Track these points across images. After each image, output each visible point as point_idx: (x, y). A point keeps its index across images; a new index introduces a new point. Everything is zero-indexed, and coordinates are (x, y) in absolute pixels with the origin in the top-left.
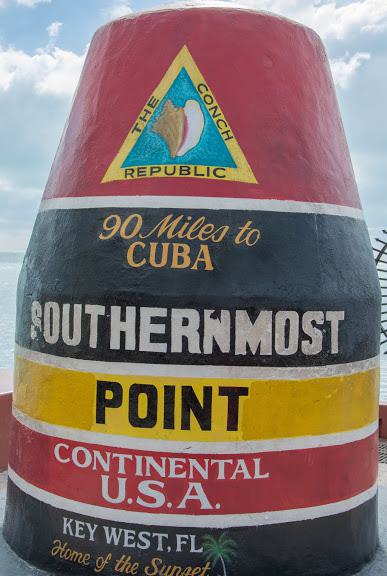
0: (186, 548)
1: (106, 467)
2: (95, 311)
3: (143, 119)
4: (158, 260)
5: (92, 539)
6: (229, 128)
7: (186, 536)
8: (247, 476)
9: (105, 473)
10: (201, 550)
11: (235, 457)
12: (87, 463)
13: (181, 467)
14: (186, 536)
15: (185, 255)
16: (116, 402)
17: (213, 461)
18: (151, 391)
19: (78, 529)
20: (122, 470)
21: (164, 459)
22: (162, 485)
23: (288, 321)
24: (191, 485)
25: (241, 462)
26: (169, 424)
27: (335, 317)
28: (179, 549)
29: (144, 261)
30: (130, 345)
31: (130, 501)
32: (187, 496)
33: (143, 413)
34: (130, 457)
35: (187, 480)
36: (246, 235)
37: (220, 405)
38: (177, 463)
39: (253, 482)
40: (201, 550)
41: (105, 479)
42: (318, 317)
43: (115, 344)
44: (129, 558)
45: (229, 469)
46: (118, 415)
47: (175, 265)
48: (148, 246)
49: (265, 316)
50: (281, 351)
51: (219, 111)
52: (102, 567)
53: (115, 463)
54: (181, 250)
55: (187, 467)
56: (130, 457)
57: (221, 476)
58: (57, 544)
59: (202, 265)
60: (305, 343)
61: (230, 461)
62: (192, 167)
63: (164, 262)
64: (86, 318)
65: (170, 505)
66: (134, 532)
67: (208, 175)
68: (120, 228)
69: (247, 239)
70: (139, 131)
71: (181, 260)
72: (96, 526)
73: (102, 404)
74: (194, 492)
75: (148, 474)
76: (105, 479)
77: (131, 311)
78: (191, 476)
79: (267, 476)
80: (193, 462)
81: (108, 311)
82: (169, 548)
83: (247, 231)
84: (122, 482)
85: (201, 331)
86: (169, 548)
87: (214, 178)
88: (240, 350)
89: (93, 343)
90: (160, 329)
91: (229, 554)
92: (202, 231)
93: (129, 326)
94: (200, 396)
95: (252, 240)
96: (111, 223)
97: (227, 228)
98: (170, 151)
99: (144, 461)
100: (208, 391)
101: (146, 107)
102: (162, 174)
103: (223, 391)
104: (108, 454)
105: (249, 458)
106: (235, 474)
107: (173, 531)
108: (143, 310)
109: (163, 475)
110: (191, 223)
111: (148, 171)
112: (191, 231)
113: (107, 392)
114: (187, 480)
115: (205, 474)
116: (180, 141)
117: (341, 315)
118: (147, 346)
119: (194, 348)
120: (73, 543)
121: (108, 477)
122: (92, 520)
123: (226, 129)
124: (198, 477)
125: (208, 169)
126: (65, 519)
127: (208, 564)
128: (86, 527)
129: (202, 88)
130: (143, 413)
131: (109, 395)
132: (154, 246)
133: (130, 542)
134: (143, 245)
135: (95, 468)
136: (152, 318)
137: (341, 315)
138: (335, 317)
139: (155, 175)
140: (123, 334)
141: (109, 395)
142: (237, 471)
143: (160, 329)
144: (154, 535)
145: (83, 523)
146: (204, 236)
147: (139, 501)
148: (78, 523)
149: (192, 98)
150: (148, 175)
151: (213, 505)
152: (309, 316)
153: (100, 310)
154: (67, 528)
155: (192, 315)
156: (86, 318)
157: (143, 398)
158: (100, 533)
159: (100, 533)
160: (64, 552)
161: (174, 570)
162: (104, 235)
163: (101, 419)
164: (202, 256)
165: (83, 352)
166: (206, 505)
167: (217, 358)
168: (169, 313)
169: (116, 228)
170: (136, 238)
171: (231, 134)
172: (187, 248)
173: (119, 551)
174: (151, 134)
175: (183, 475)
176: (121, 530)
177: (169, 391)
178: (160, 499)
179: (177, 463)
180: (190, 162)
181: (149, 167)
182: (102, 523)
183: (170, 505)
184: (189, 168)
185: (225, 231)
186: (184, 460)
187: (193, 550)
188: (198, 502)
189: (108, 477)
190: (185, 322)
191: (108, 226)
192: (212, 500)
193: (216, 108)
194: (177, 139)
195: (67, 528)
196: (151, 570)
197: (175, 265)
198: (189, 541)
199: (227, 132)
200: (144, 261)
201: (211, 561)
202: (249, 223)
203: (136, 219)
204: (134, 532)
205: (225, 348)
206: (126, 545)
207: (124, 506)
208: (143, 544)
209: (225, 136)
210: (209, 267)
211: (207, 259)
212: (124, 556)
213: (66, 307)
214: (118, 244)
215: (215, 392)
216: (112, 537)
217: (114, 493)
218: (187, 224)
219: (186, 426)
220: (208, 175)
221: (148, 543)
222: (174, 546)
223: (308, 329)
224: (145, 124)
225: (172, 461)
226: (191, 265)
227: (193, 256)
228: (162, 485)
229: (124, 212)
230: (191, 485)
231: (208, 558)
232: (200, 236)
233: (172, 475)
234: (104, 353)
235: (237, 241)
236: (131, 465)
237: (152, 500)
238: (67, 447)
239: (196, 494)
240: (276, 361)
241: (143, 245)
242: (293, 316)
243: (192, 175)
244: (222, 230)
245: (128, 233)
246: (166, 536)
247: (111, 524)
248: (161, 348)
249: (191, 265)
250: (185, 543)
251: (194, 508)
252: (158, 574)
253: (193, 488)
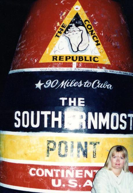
2: (46, 113)
64: (42, 117)
73: (49, 150)
87: (94, 62)
89: (46, 126)
152: (122, 115)
156: (42, 117)
165: (41, 129)
205: (95, 127)
213: (32, 113)
242: (116, 115)
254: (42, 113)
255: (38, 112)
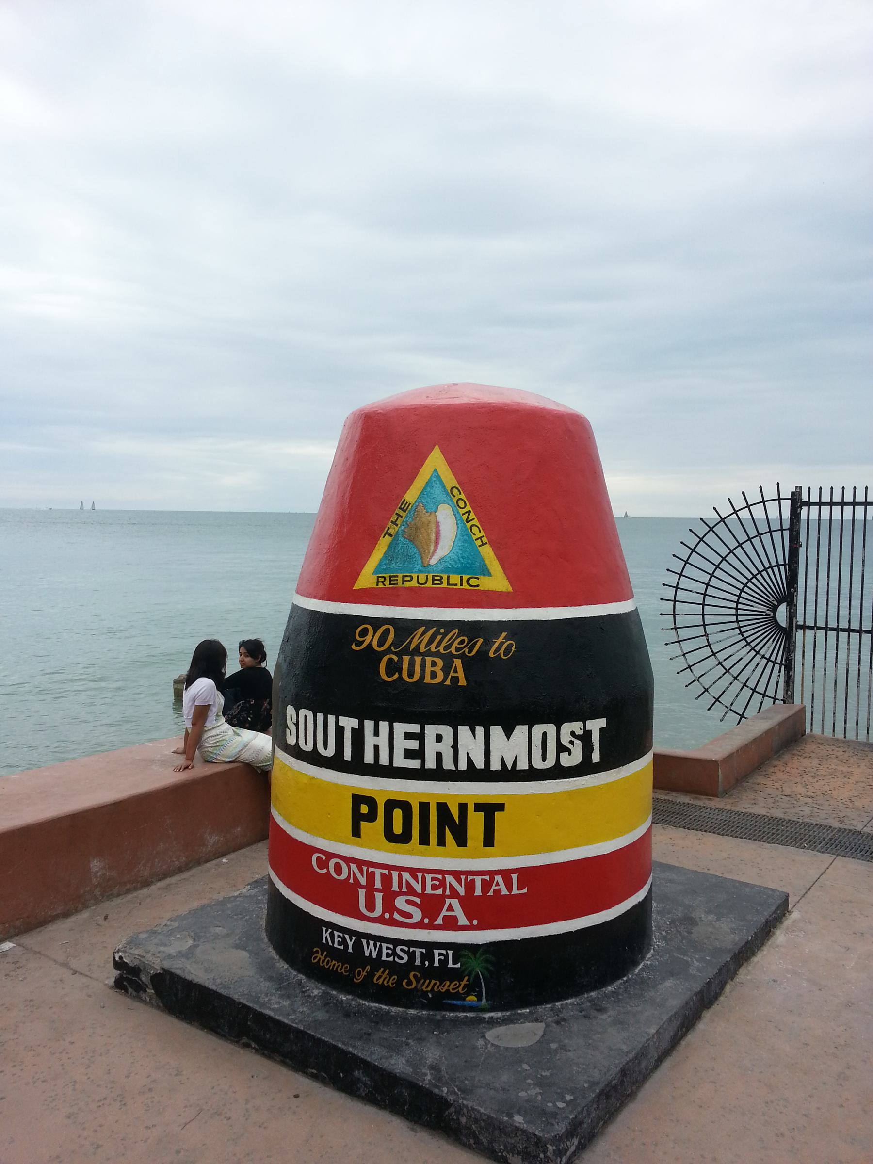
0: (444, 962)
1: (363, 881)
2: (349, 723)
3: (394, 523)
4: (411, 674)
5: (350, 950)
6: (482, 534)
7: (444, 952)
8: (505, 892)
9: (362, 887)
10: (458, 965)
11: (492, 873)
12: (344, 876)
13: (437, 883)
14: (444, 952)
15: (438, 669)
16: (371, 817)
17: (470, 878)
18: (405, 806)
19: (336, 940)
20: (378, 884)
21: (420, 875)
22: (418, 900)
23: (545, 734)
24: (448, 901)
25: (498, 878)
26: (424, 840)
27: (596, 725)
28: (436, 964)
29: (396, 676)
30: (384, 760)
31: (387, 916)
32: (444, 913)
33: (398, 829)
34: (386, 872)
35: (443, 897)
36: (500, 646)
37: (476, 822)
38: (433, 879)
39: (511, 896)
40: (458, 965)
41: (362, 893)
42: (577, 727)
43: (369, 758)
44: (388, 971)
45: (486, 885)
46: (374, 829)
47: (428, 680)
48: (401, 661)
49: (521, 731)
50: (538, 764)
51: (472, 515)
52: (361, 978)
53: (371, 877)
54: (434, 664)
55: (443, 883)
56: (386, 872)
57: (478, 892)
58: (317, 952)
59: (455, 680)
60: (564, 756)
61: (487, 878)
62: (445, 577)
63: (417, 677)
64: (340, 730)
65: (426, 921)
66: (391, 946)
67: (461, 585)
68: (372, 638)
69: (502, 652)
70: (390, 535)
71: (434, 675)
72: (354, 938)
73: (357, 819)
74: (450, 908)
75: (404, 889)
76: (362, 893)
77: (384, 726)
78: (448, 893)
79: (525, 891)
80: (449, 879)
81: (362, 725)
82: (427, 963)
83: (502, 644)
84: (379, 897)
85: (455, 747)
86: (427, 963)
88: (495, 766)
89: (348, 755)
90: (414, 745)
91: (487, 969)
92: (455, 644)
93: (383, 741)
94: (455, 812)
95: (508, 650)
96: (364, 633)
97: (481, 640)
98: (422, 558)
99: (400, 877)
100: (463, 807)
101: (397, 511)
102: (413, 584)
103: (479, 807)
104: (365, 868)
105: (506, 874)
106: (492, 890)
107: (431, 946)
108: (396, 725)
109: (419, 890)
110: (444, 635)
111: (400, 579)
112: (444, 644)
113: (362, 805)
114: (443, 897)
115: (461, 891)
116: (432, 548)
117: (602, 722)
118: (400, 762)
119: (448, 764)
120: (332, 952)
121: (364, 891)
122: (351, 932)
123: (479, 535)
124: (454, 894)
125: (461, 577)
126: (324, 929)
127: (466, 978)
128: (344, 939)
129: (455, 491)
130: (398, 829)
131: (364, 809)
132: (406, 659)
133: (388, 955)
134: (396, 658)
135: (351, 881)
136: (405, 733)
137: (602, 722)
138: (596, 725)
139: (407, 584)
140: (376, 748)
141: (364, 809)
142: (494, 887)
143: (414, 745)
144: (412, 949)
145: (341, 935)
146: (457, 649)
147: (396, 916)
148: (336, 933)
149: (444, 502)
150: (400, 585)
151: (471, 922)
152: (567, 728)
153: (354, 723)
154: (326, 937)
155: (446, 731)
156: (340, 730)
157: (398, 814)
158: (358, 946)
159: (358, 946)
160: (323, 961)
161: (432, 984)
162: (356, 646)
163: (356, 832)
164: (456, 671)
165: (336, 763)
166: (463, 921)
167: (472, 774)
168: (423, 729)
169: (368, 639)
170: (388, 651)
171: (485, 540)
172: (440, 663)
173: (377, 963)
174: (402, 539)
175: (440, 892)
176: (378, 944)
177: (424, 807)
178: (417, 915)
179: (433, 879)
180: (442, 572)
181: (400, 575)
182: (359, 935)
183: (426, 921)
184: (442, 578)
185: (479, 644)
186: (440, 877)
187: (450, 965)
188: (455, 918)
189: (364, 891)
190: (439, 738)
191: (360, 636)
192: (470, 918)
193: (470, 511)
194: (428, 546)
195: (326, 937)
196: (410, 983)
197: (428, 680)
198: (446, 956)
199: (481, 538)
200: (396, 676)
201: (469, 975)
202: (504, 634)
203: (387, 631)
204: (391, 946)
205: (480, 764)
206: (384, 958)
207: (380, 920)
208: (401, 958)
209: (479, 542)
210: (463, 682)
211: (461, 674)
212: (382, 969)
214: (371, 656)
215: (471, 808)
216: (370, 949)
217: (371, 907)
218: (439, 637)
219: (441, 842)
220: (461, 585)
221: (406, 958)
222: (432, 961)
223: (565, 742)
224: (397, 528)
225: (428, 877)
226: (445, 679)
227: (446, 669)
228: (418, 900)
229: (376, 623)
230: (448, 901)
231: (466, 973)
232: (453, 650)
233: (429, 891)
234: (357, 766)
235: (491, 655)
236: (387, 880)
237: (409, 916)
238: (324, 857)
239: (453, 911)
240: (533, 775)
241: (396, 658)
242: (551, 729)
243: (445, 585)
244: (475, 643)
245: (381, 643)
246: (424, 951)
247: (369, 937)
248: (415, 764)
249: (445, 679)
250: (442, 958)
251: (451, 924)
252: (416, 987)
253: (450, 903)
254: (344, 721)
255: (331, 719)
